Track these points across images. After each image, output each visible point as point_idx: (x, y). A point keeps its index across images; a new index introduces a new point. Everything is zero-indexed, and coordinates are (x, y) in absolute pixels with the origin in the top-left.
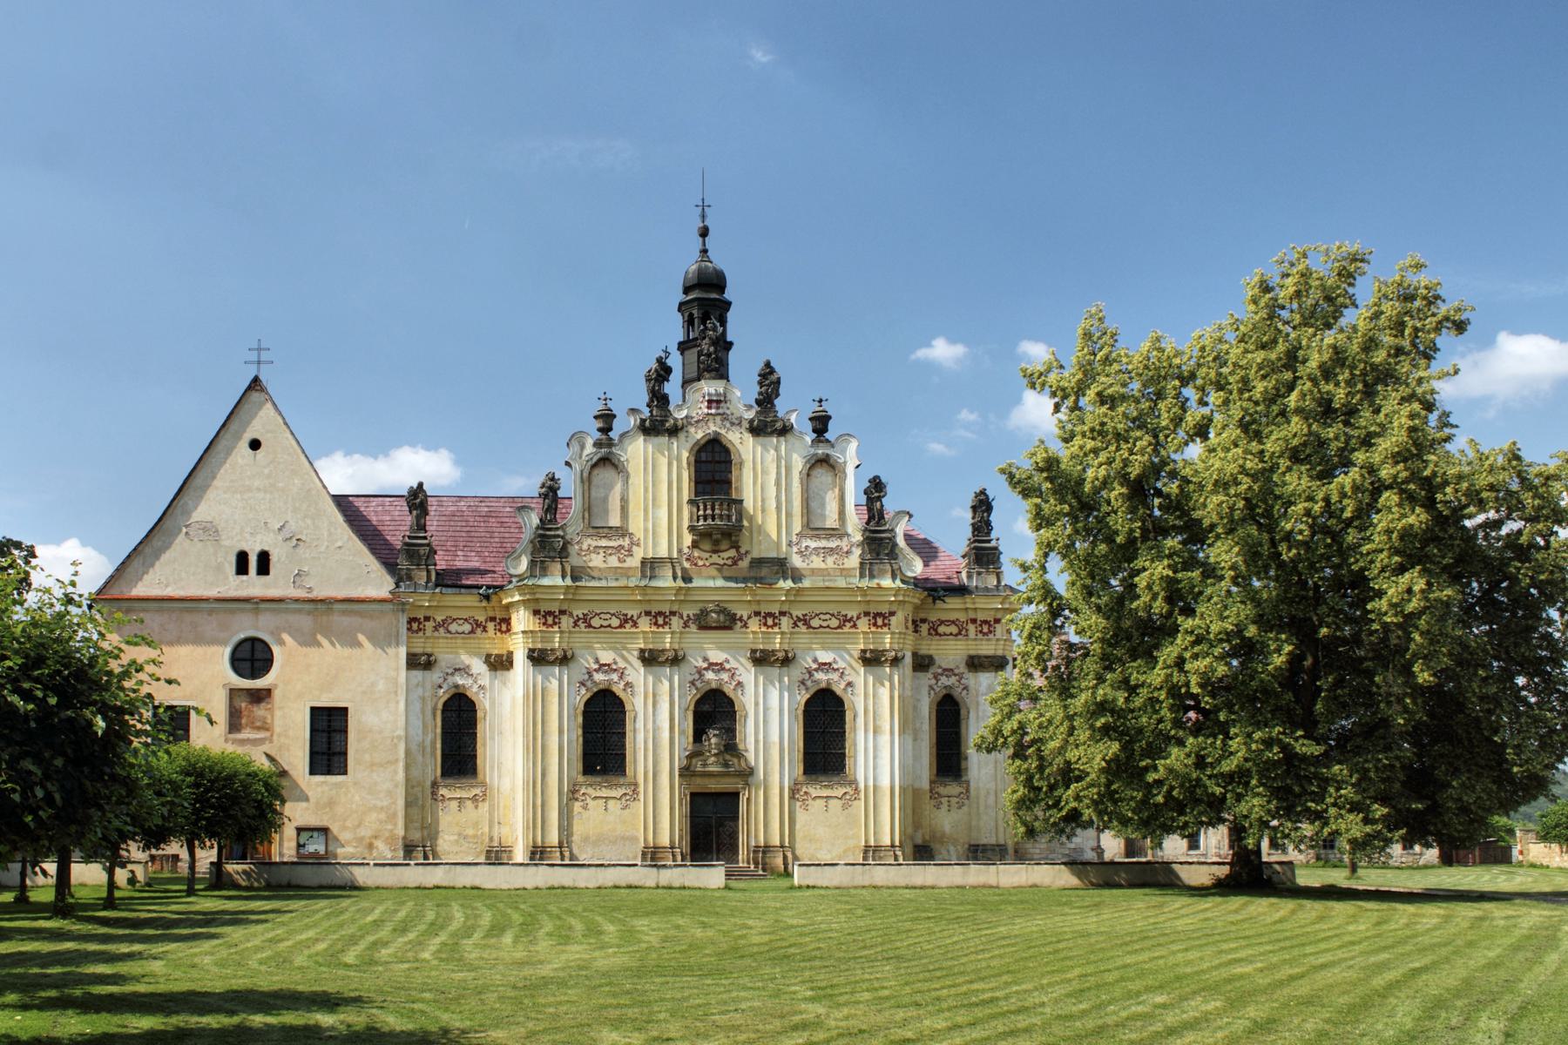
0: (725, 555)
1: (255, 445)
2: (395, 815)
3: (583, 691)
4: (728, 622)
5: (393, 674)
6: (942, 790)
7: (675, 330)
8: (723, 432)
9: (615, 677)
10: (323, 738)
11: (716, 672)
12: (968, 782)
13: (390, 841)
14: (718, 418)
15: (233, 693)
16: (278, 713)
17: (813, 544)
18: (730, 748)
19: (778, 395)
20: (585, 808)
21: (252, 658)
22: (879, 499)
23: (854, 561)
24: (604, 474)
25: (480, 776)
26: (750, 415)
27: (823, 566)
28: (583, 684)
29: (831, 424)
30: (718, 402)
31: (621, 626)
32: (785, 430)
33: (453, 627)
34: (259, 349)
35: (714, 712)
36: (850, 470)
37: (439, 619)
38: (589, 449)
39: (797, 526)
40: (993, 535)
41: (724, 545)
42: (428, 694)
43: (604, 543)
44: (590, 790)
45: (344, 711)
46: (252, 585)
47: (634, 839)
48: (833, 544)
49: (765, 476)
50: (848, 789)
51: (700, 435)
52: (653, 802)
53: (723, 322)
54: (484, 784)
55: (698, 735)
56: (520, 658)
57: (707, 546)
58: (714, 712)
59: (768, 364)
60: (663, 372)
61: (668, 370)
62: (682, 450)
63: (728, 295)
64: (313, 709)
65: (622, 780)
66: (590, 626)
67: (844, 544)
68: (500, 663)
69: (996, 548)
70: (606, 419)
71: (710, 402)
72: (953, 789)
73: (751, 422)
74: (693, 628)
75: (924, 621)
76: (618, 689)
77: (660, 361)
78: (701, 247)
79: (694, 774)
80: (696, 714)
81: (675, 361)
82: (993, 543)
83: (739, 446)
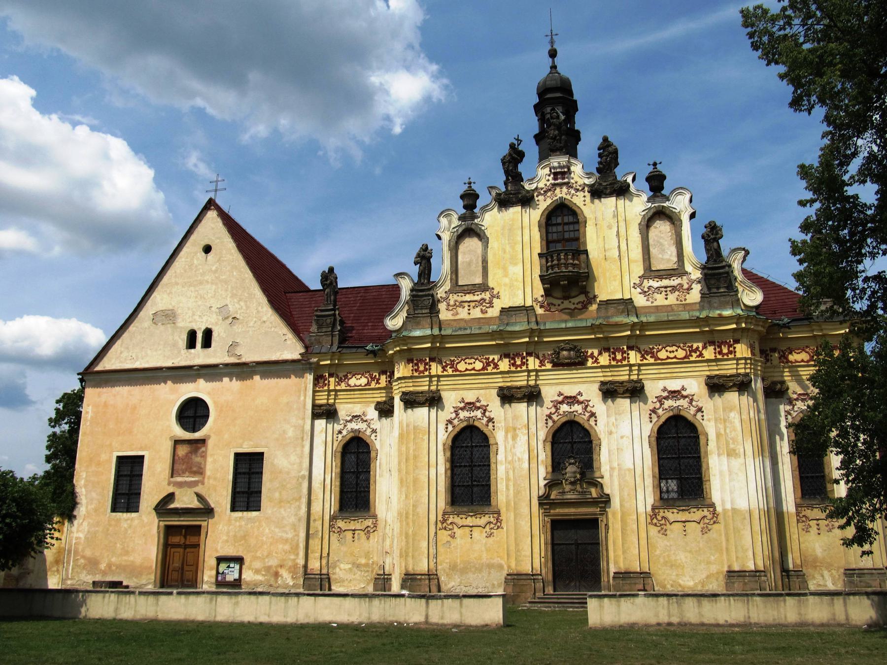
0: (576, 300)
1: (207, 249)
2: (297, 546)
3: (450, 428)
5: (300, 422)
6: (808, 513)
8: (568, 197)
9: (478, 414)
10: (243, 480)
11: (570, 404)
13: (293, 570)
15: (177, 442)
16: (209, 459)
17: (655, 284)
19: (617, 164)
20: (453, 536)
21: (193, 413)
22: (716, 240)
23: (695, 295)
24: (471, 245)
25: (372, 510)
27: (666, 303)
29: (666, 183)
30: (563, 173)
31: (484, 368)
32: (622, 191)
33: (353, 381)
35: (572, 444)
36: (685, 218)
38: (456, 222)
39: (639, 270)
42: (329, 439)
43: (468, 297)
44: (457, 520)
45: (261, 454)
49: (612, 232)
50: (706, 512)
51: (549, 201)
54: (375, 517)
55: (557, 465)
57: (558, 294)
58: (572, 444)
59: (605, 139)
60: (514, 157)
61: (521, 155)
62: (535, 215)
64: (238, 456)
65: (486, 510)
67: (684, 281)
68: (385, 410)
70: (470, 198)
71: (556, 174)
73: (591, 186)
74: (549, 366)
75: (774, 350)
76: (481, 424)
77: (512, 146)
79: (554, 504)
81: (531, 149)
83: (583, 208)
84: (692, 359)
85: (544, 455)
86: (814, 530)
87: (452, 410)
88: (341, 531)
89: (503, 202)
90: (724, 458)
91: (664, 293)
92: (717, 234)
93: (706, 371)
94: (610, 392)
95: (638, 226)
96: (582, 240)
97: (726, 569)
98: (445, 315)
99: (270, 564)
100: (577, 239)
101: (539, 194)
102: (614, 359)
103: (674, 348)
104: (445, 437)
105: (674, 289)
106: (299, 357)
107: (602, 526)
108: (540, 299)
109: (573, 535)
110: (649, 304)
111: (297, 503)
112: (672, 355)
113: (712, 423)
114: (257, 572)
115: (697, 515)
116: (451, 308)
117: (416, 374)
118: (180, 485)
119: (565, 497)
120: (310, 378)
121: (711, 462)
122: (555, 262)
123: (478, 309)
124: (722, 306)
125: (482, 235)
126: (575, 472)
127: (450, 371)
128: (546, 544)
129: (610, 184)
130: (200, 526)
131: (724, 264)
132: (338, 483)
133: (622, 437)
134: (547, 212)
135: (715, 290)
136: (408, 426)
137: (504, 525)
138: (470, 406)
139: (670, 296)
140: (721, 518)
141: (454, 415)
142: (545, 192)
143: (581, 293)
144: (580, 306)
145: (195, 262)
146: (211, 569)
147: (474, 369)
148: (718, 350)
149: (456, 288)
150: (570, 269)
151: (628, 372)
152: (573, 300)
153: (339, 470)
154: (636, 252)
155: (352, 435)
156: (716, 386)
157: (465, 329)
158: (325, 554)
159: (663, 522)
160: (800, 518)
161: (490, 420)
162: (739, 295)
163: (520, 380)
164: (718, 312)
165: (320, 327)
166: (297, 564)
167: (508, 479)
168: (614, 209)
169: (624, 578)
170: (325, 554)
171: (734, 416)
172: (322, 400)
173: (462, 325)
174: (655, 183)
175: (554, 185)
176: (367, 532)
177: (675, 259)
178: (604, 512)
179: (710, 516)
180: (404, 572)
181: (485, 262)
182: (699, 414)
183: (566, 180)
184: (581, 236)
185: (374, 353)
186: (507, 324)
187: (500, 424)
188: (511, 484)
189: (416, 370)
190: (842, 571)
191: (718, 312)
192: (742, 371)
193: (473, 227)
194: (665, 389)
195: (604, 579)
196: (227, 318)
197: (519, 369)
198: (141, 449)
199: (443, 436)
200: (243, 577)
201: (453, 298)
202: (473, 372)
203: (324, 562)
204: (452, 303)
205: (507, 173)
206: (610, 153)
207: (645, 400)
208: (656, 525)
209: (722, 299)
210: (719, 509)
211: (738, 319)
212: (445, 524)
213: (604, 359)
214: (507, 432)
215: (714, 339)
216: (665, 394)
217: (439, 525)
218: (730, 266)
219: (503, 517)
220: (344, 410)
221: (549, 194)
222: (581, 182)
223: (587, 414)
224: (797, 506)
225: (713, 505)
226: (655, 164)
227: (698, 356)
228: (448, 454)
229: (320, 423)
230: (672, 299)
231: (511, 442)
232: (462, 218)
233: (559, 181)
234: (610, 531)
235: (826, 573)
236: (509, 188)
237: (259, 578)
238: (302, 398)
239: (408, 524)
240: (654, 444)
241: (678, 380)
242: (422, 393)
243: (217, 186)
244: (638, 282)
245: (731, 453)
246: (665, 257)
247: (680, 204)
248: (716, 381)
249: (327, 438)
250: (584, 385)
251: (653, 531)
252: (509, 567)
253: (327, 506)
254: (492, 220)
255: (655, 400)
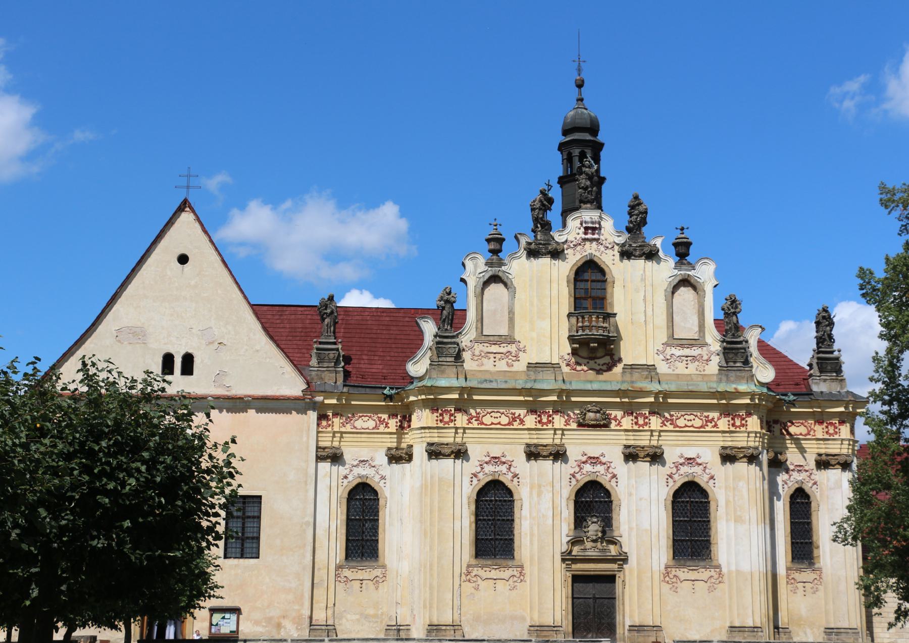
0: (601, 361)
1: (183, 259)
2: (302, 596)
3: (475, 481)
4: (603, 425)
6: (797, 576)
7: (556, 167)
8: (597, 254)
9: (503, 468)
12: (820, 569)
13: (297, 621)
14: (594, 243)
17: (678, 352)
18: (607, 536)
20: (477, 589)
22: (735, 314)
23: (713, 367)
26: (621, 240)
27: (687, 372)
28: (475, 475)
29: (692, 249)
30: (594, 229)
31: (509, 424)
32: (651, 255)
34: (189, 176)
36: (709, 289)
40: (836, 347)
41: (600, 353)
42: (334, 484)
43: (495, 349)
44: (481, 572)
47: (523, 619)
48: (695, 352)
50: (713, 572)
51: (578, 256)
52: (538, 586)
53: (597, 160)
54: (384, 567)
55: (579, 522)
56: (419, 452)
57: (584, 353)
61: (551, 201)
62: (563, 269)
63: (600, 138)
65: (510, 563)
66: (482, 423)
67: (704, 352)
69: (837, 359)
71: (586, 229)
72: (807, 575)
73: (623, 245)
74: (574, 426)
78: (576, 96)
79: (575, 561)
80: (576, 502)
81: (556, 193)
82: (836, 353)
83: (611, 267)
84: (707, 429)
85: (568, 513)
86: (800, 591)
87: (478, 463)
88: (347, 580)
89: (533, 253)
90: (732, 524)
91: (685, 362)
92: (736, 307)
93: (720, 441)
94: (631, 456)
95: (663, 293)
96: (609, 300)
97: (728, 624)
98: (469, 364)
99: (271, 614)
100: (603, 299)
101: (569, 247)
102: (636, 423)
103: (692, 417)
104: (470, 490)
105: (694, 358)
106: (300, 394)
107: (619, 581)
108: (567, 357)
109: (590, 590)
110: (670, 371)
112: (689, 424)
113: (723, 491)
114: (257, 623)
115: (704, 574)
116: (476, 358)
117: (441, 425)
119: (587, 554)
120: (313, 415)
121: (719, 526)
122: (586, 324)
123: (504, 362)
124: (739, 379)
125: (509, 283)
126: (597, 531)
127: (475, 424)
128: (567, 597)
129: (640, 246)
131: (741, 339)
132: (344, 531)
133: (641, 499)
134: (576, 267)
135: (731, 364)
136: (432, 477)
137: (527, 578)
138: (496, 460)
139: (691, 366)
140: (725, 578)
141: (479, 469)
142: (575, 246)
143: (606, 355)
144: (604, 368)
145: (169, 273)
146: (203, 620)
147: (499, 423)
148: (732, 422)
149: (483, 338)
150: (601, 332)
151: (649, 437)
152: (598, 361)
153: (345, 517)
154: (661, 319)
155: (359, 480)
156: (728, 457)
157: (491, 381)
158: (330, 605)
159: (674, 580)
160: (790, 580)
161: (515, 476)
162: (754, 370)
163: (546, 438)
164: (734, 386)
165: (320, 360)
166: (302, 615)
167: (532, 535)
168: (642, 272)
169: (638, 631)
170: (330, 605)
171: (742, 485)
172: (326, 442)
173: (488, 377)
174: (682, 250)
175: (585, 240)
176: (376, 581)
177: (697, 329)
178: (621, 568)
179: (716, 576)
180: (428, 623)
181: (511, 312)
182: (712, 481)
183: (596, 236)
184: (608, 296)
185: (390, 398)
186: (535, 381)
187: (525, 479)
188: (536, 539)
189: (441, 421)
190: (822, 629)
191: (734, 386)
192: (751, 444)
193: (500, 274)
194: (681, 456)
195: (619, 631)
196: (212, 343)
197: (545, 427)
199: (468, 490)
200: (240, 629)
201: (478, 348)
202: (498, 426)
203: (330, 612)
204: (477, 353)
205: (536, 220)
206: (641, 213)
207: (663, 463)
208: (668, 582)
209: (738, 373)
210: (725, 570)
211: (752, 395)
212: (469, 577)
213: (627, 422)
214: (531, 488)
215: (728, 411)
216: (682, 461)
217: (463, 577)
218: (747, 342)
219: (527, 570)
220: (350, 453)
221: (579, 248)
222: (611, 239)
223: (609, 476)
224: (788, 569)
225: (718, 567)
226: (682, 229)
227: (714, 427)
228: (473, 507)
229: (325, 466)
230: (692, 368)
231: (535, 499)
232: (489, 264)
233: (589, 236)
234: (627, 586)
235: (808, 631)
236: (539, 237)
237: (259, 629)
238: (305, 439)
239: (431, 575)
240: (670, 507)
241: (694, 448)
242: (447, 444)
243: (188, 181)
244: (661, 349)
245: (738, 520)
246: (687, 327)
247: (705, 273)
248: (728, 452)
249: (333, 483)
250: (608, 446)
251: (666, 587)
252: (532, 619)
253: (332, 554)
254: (519, 267)
255: (672, 465)
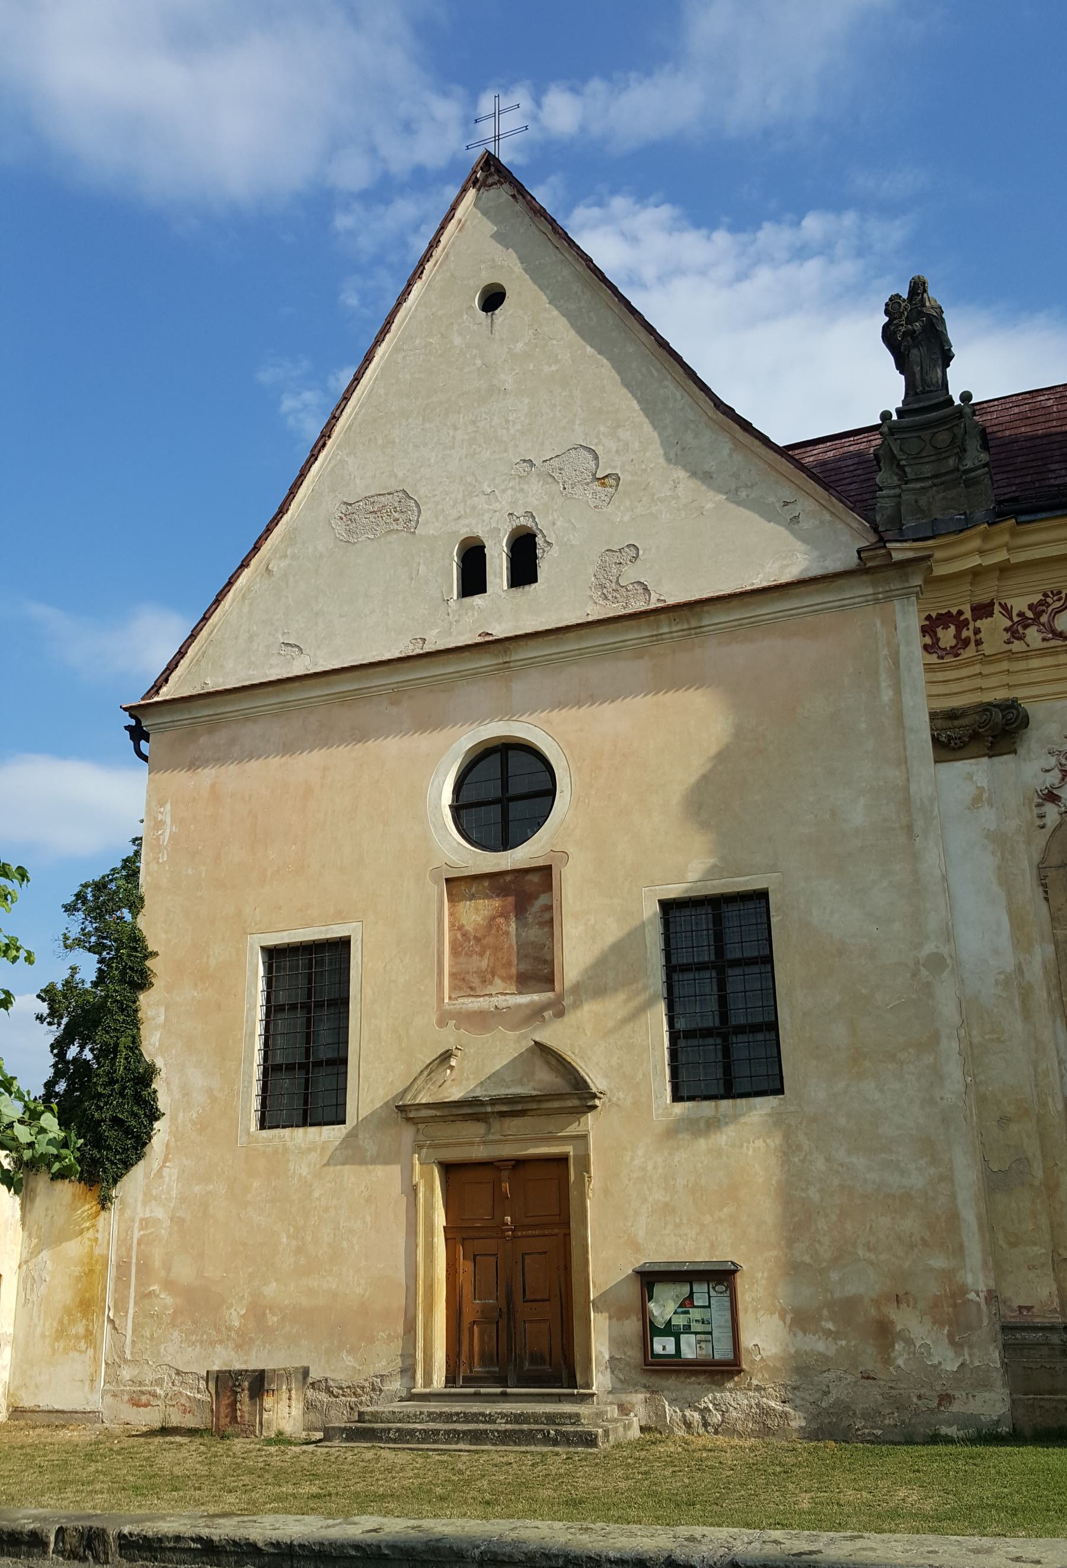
2: (954, 1218)
13: (953, 1314)
15: (458, 885)
21: (505, 791)
37: (1020, 604)
46: (501, 609)
99: (851, 1289)
111: (928, 1059)
118: (481, 1020)
130: (562, 1160)
145: (457, 341)
166: (963, 1290)
198: (340, 917)
229: (971, 773)
238: (887, 695)
